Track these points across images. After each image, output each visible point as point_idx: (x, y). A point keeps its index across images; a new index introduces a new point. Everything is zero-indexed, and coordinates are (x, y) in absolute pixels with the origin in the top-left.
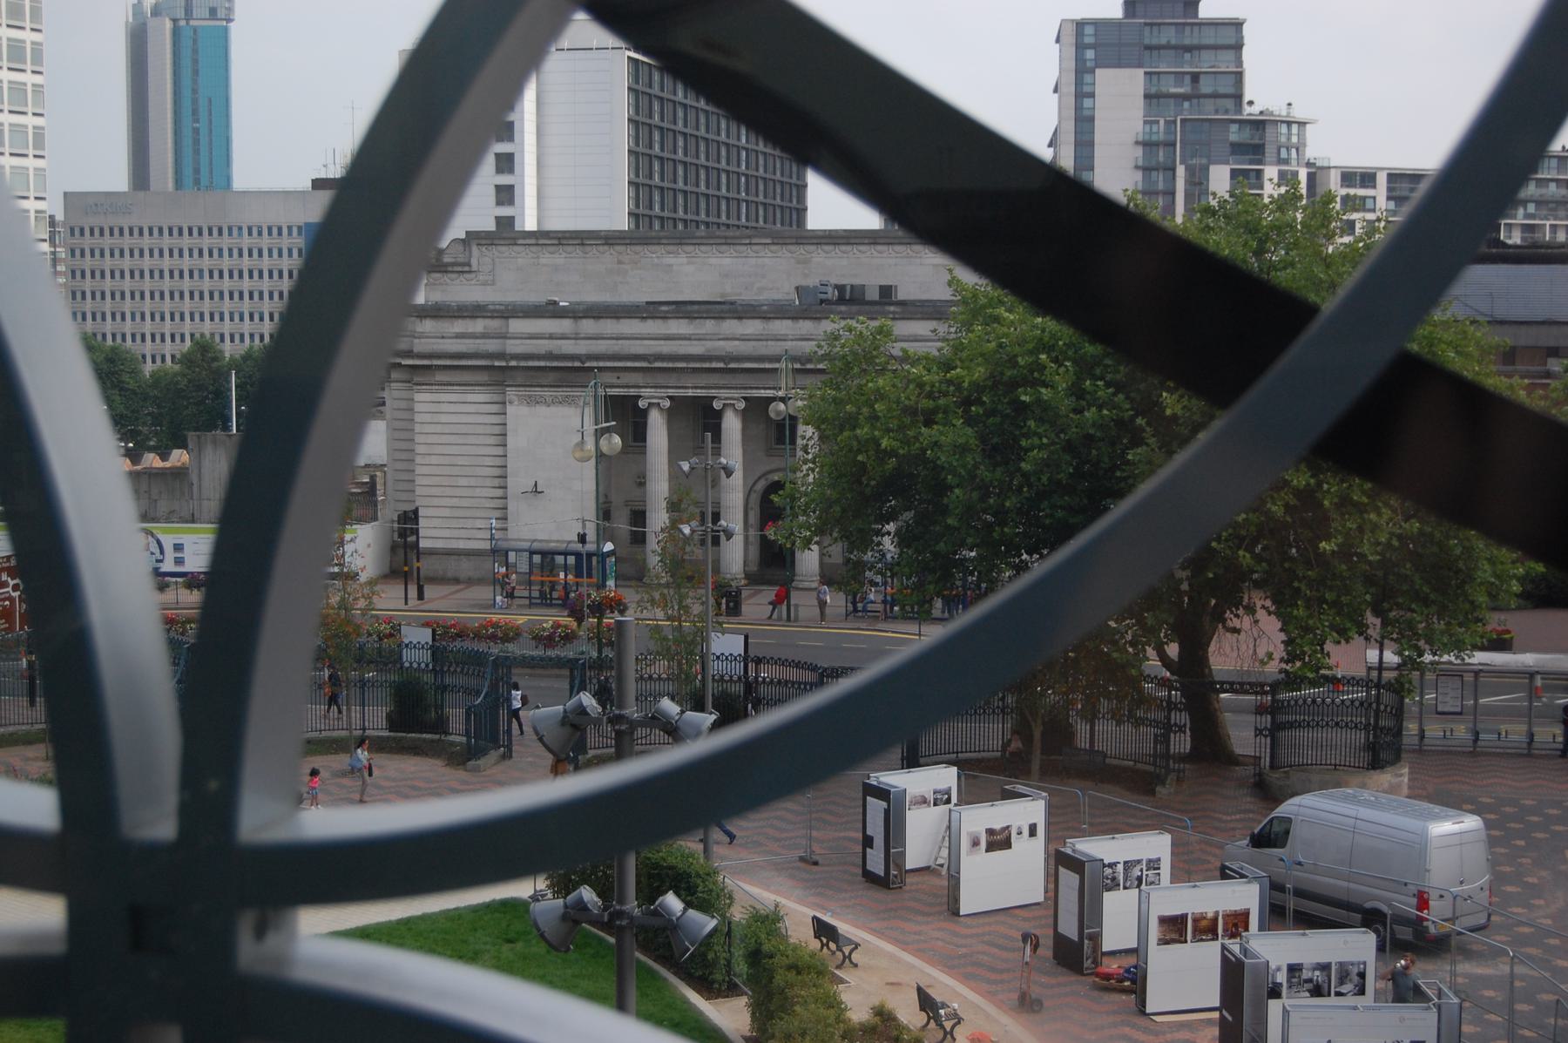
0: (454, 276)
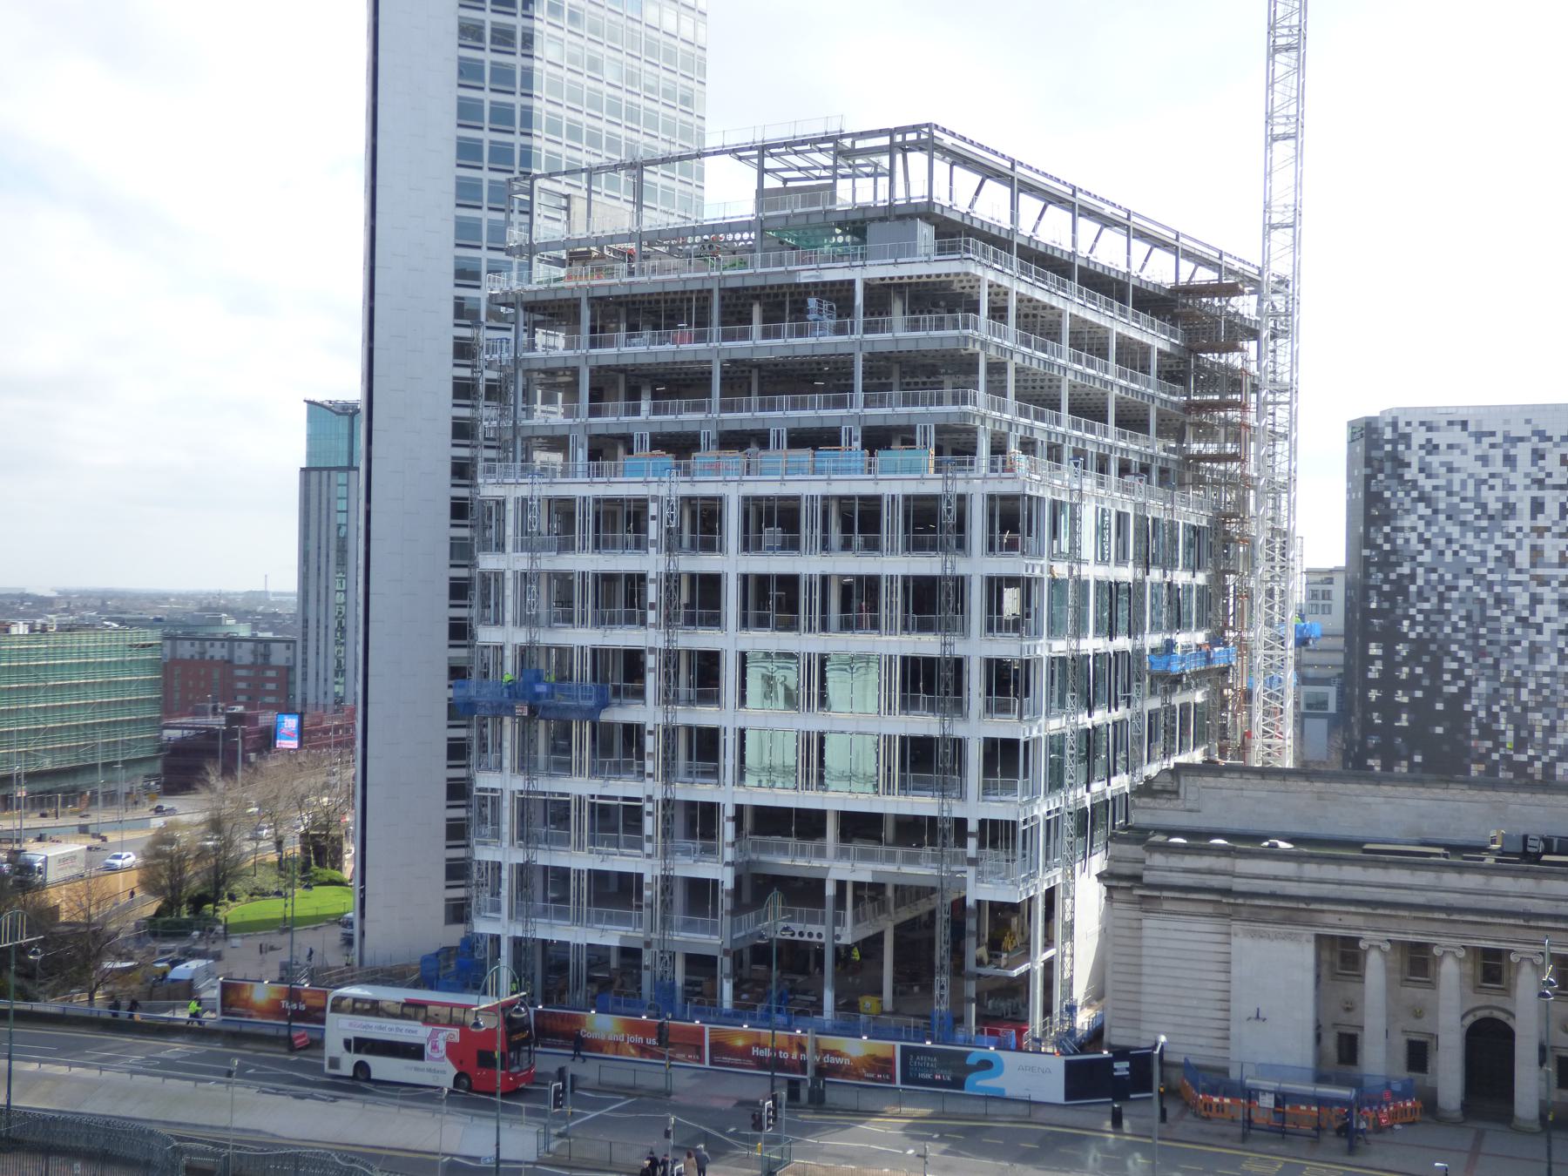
0: (1162, 801)
